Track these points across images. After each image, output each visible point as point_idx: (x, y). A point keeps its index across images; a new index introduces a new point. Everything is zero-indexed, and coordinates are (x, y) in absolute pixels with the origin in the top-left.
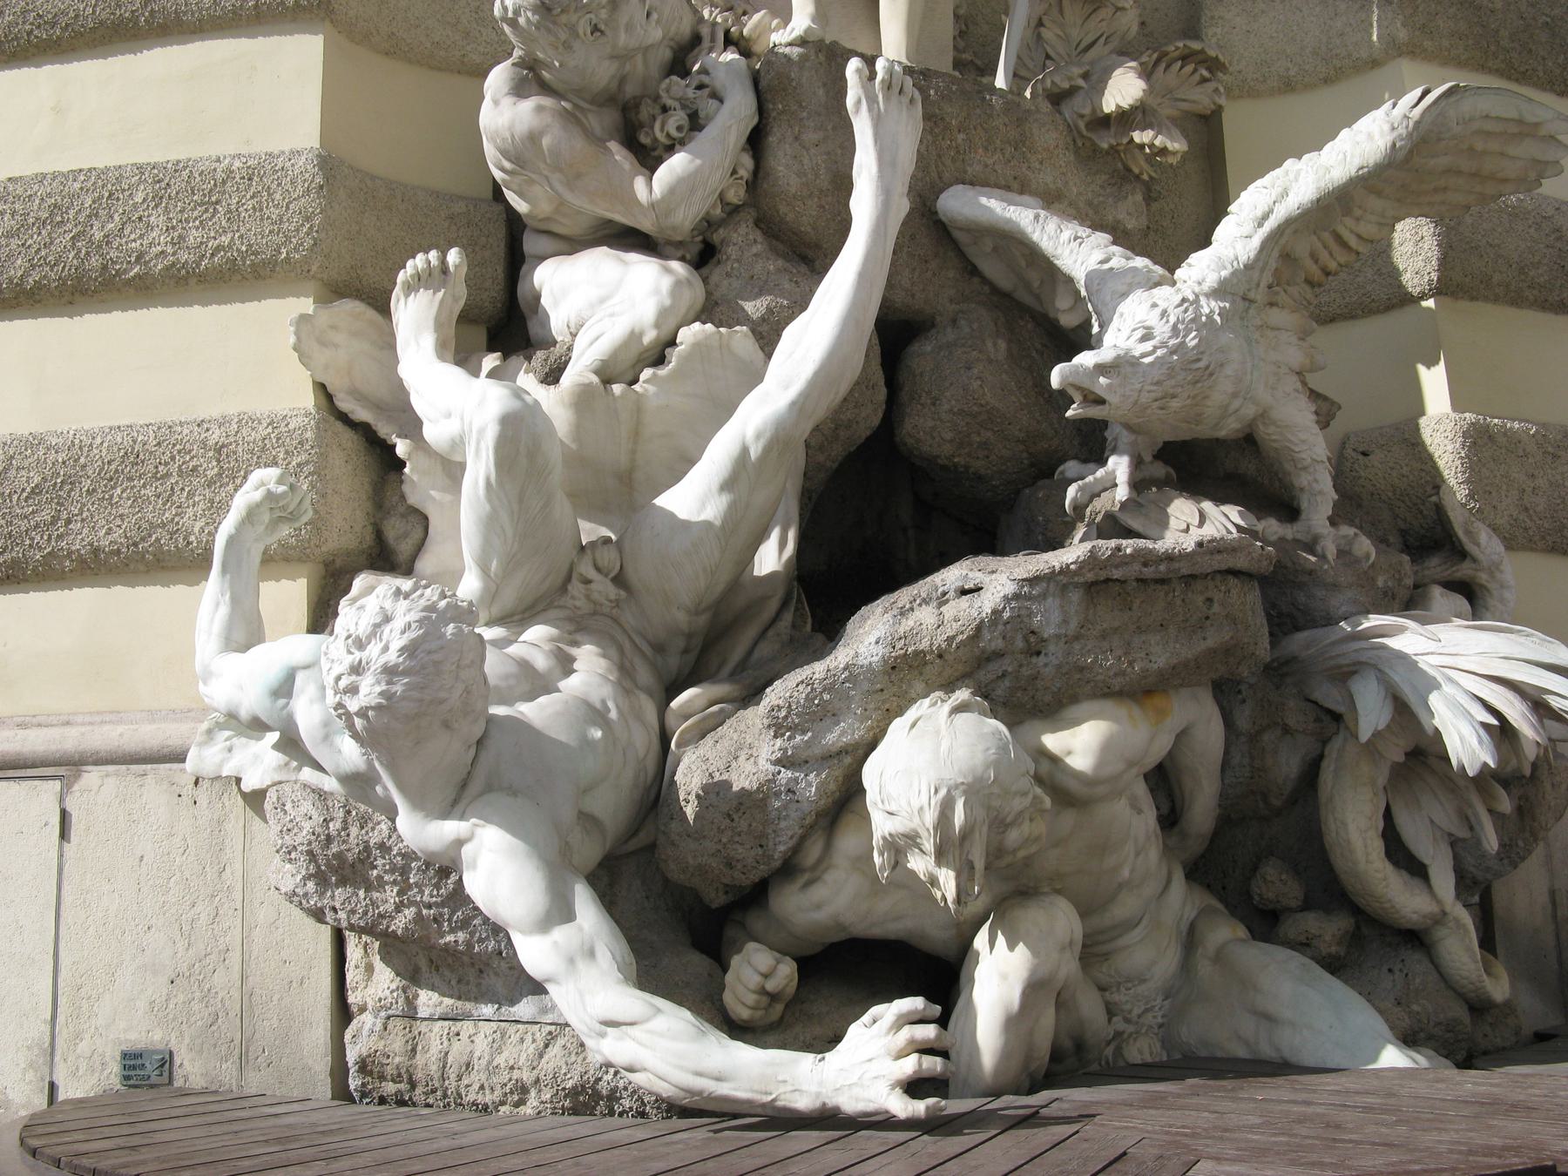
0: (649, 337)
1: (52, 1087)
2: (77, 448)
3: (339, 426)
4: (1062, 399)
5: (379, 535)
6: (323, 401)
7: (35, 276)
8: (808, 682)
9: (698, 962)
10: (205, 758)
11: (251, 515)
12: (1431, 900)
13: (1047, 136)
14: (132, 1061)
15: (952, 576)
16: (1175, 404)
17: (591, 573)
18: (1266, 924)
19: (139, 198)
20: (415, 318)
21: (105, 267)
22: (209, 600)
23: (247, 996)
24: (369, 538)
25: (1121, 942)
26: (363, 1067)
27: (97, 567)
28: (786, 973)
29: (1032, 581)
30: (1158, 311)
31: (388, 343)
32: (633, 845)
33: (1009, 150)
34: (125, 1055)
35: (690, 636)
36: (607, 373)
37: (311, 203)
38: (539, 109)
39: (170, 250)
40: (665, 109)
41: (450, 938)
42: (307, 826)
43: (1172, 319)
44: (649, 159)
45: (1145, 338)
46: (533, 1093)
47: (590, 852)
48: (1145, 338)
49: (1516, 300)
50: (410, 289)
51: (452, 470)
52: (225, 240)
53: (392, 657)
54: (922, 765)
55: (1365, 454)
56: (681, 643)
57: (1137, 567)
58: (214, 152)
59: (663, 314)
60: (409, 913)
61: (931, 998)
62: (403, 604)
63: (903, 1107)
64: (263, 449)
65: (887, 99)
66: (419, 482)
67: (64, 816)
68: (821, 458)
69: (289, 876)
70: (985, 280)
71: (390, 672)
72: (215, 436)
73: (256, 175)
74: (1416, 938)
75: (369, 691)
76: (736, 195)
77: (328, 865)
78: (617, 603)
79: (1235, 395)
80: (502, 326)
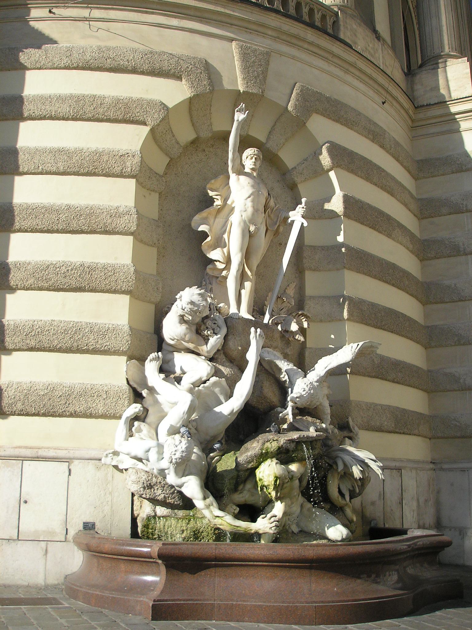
8: (247, 456)
21: (78, 346)
34: (84, 523)
37: (128, 338)
39: (94, 344)
40: (207, 328)
41: (170, 501)
42: (144, 478)
44: (206, 340)
46: (185, 532)
49: (364, 375)
50: (151, 361)
54: (268, 472)
59: (208, 374)
60: (163, 495)
64: (117, 393)
67: (70, 470)
70: (263, 367)
71: (183, 452)
72: (105, 389)
73: (115, 330)
75: (178, 455)
77: (147, 486)
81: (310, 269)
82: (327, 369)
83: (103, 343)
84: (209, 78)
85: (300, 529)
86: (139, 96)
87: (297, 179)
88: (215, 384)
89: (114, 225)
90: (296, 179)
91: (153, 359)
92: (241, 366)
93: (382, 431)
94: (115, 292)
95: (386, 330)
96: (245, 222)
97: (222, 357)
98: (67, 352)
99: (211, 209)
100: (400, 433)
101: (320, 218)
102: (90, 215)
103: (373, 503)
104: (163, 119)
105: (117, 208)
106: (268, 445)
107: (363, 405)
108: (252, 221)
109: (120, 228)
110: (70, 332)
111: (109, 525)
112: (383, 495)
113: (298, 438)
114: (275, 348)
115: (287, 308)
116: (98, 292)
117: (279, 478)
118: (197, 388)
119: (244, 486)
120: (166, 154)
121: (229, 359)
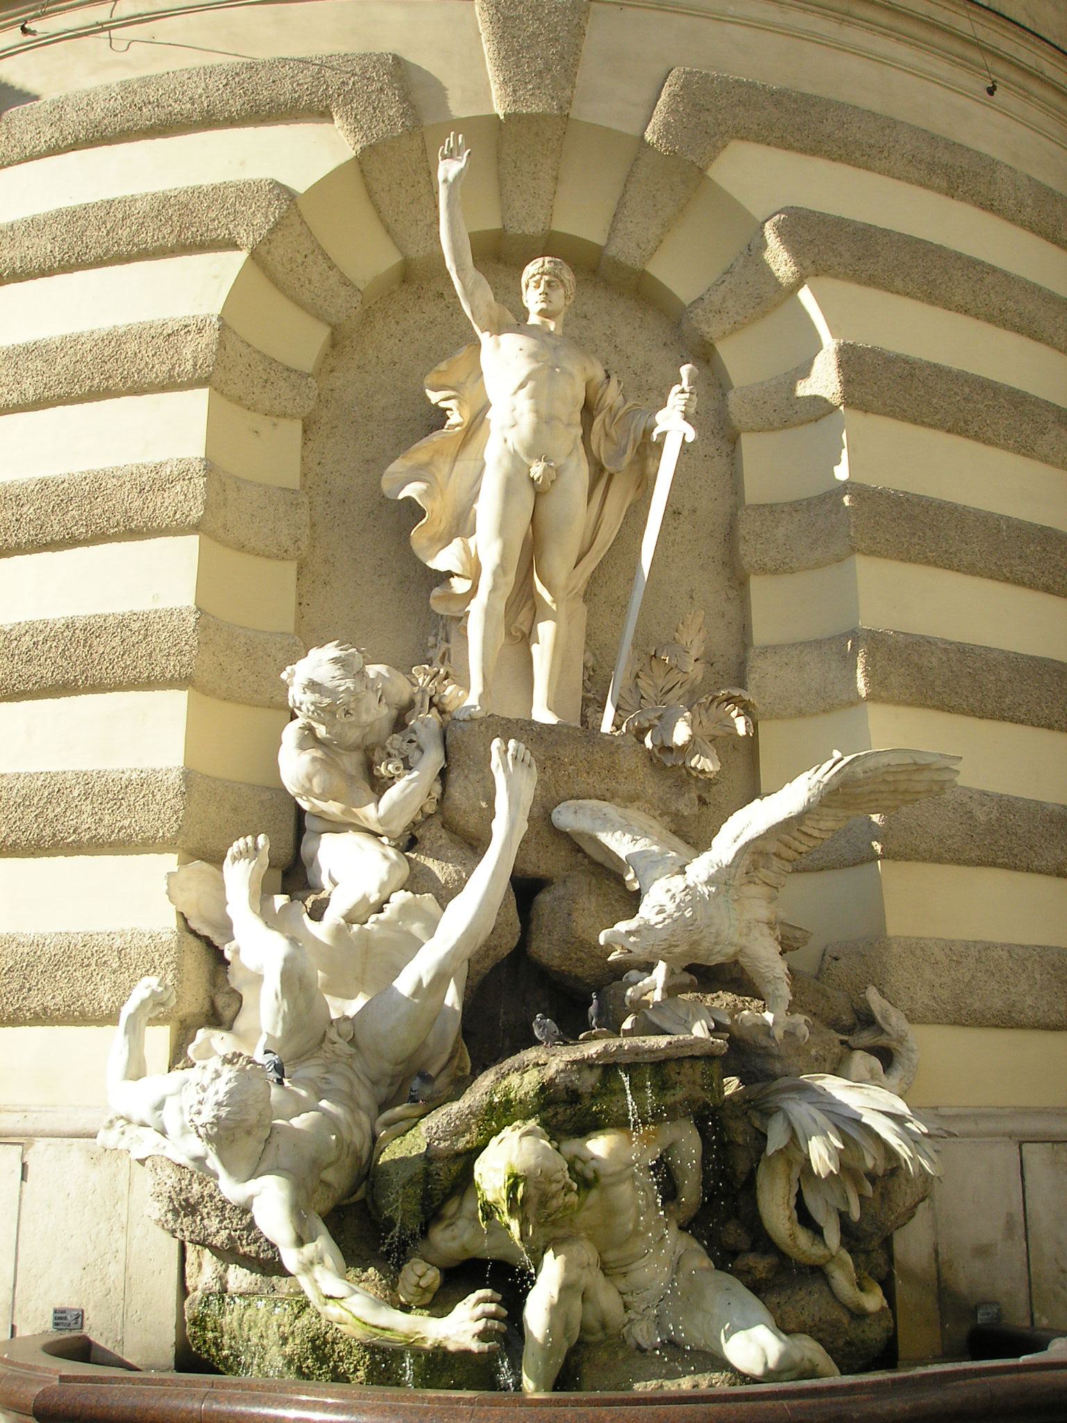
0: (374, 898)
1: (13, 1327)
2: (37, 946)
3: (191, 938)
4: (609, 949)
5: (213, 1004)
6: (182, 923)
10: (108, 1138)
11: (143, 1003)
13: (629, 761)
16: (677, 950)
17: (335, 1037)
18: (724, 1258)
21: (54, 835)
23: (127, 1279)
24: (207, 1006)
25: (634, 1266)
26: (194, 1322)
27: (42, 1018)
29: (573, 1062)
30: (670, 894)
32: (353, 1200)
33: (604, 773)
34: (55, 1312)
35: (393, 1077)
36: (350, 919)
37: (178, 803)
38: (314, 759)
39: (93, 827)
40: (389, 755)
41: (247, 1249)
42: (169, 1182)
43: (678, 900)
44: (379, 786)
45: (658, 913)
46: (291, 1339)
47: (327, 1205)
48: (658, 913)
49: (939, 860)
50: (235, 859)
51: (258, 979)
52: (126, 823)
53: (221, 1097)
55: (836, 959)
56: (389, 1081)
57: (632, 1056)
58: (121, 767)
59: (383, 886)
60: (224, 1233)
61: (496, 1290)
62: (228, 1066)
63: (475, 1346)
65: (514, 765)
66: (236, 979)
68: (478, 967)
69: (158, 1209)
70: (586, 856)
71: (219, 1104)
72: (118, 943)
73: (145, 783)
75: (208, 1115)
76: (430, 809)
77: (180, 1205)
78: (351, 1056)
79: (716, 943)
80: (293, 875)
81: (763, 570)
82: (741, 842)
84: (404, 99)
86: (217, 181)
87: (711, 330)
88: (404, 909)
89: (147, 513)
90: (704, 328)
91: (241, 855)
93: (1019, 1026)
94: (149, 684)
95: (1022, 722)
96: (514, 455)
97: (433, 834)
98: (33, 855)
99: (436, 436)
101: (786, 424)
102: (92, 495)
104: (277, 224)
105: (157, 468)
106: (514, 1079)
107: (936, 950)
108: (535, 449)
109: (164, 519)
110: (36, 799)
111: (118, 1319)
113: (599, 1056)
114: (631, 799)
115: (687, 687)
116: (111, 690)
117: (525, 1179)
120: (319, 317)
121: (435, 836)
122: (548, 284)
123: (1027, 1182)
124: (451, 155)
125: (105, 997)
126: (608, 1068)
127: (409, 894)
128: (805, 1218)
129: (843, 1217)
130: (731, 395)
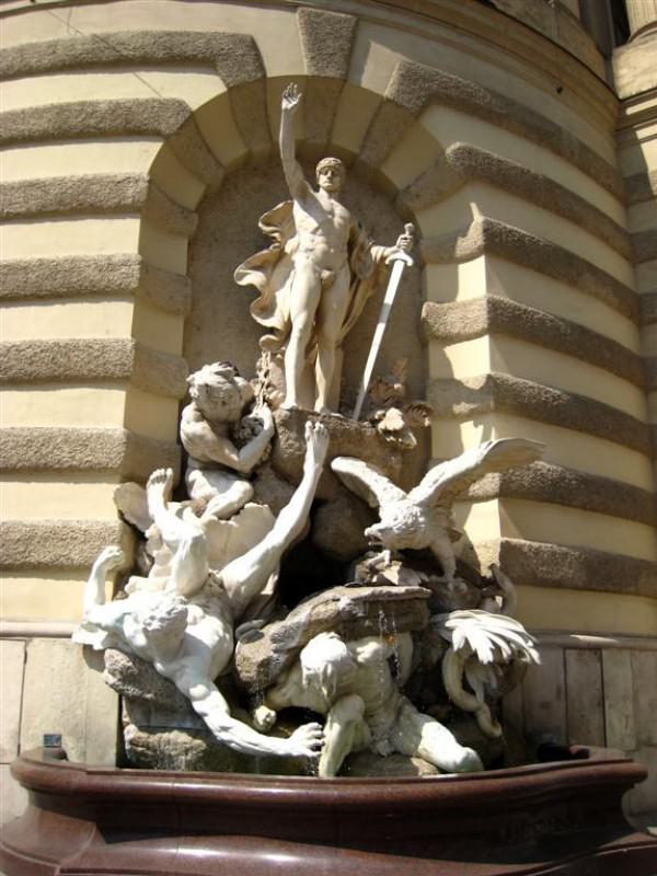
1: (19, 746)
4: (369, 538)
7: (20, 464)
9: (244, 712)
12: (476, 702)
14: (48, 738)
15: (328, 594)
17: (212, 583)
19: (59, 440)
20: (156, 492)
22: (90, 587)
24: (132, 564)
28: (273, 713)
31: (145, 497)
37: (122, 448)
40: (243, 428)
44: (239, 444)
45: (395, 520)
50: (153, 482)
52: (90, 458)
67: (26, 654)
70: (345, 487)
71: (162, 620)
72: (84, 527)
74: (472, 715)
75: (156, 625)
76: (264, 459)
80: (179, 492)
83: (83, 457)
85: (393, 749)
89: (104, 283)
92: (293, 480)
100: (600, 591)
102: (71, 270)
103: (546, 705)
112: (564, 692)
118: (223, 522)
119: (288, 676)
122: (333, 173)
123: (568, 668)
124: (291, 95)
125: (76, 557)
126: (371, 603)
127: (255, 505)
128: (466, 686)
129: (486, 686)
130: (422, 242)
